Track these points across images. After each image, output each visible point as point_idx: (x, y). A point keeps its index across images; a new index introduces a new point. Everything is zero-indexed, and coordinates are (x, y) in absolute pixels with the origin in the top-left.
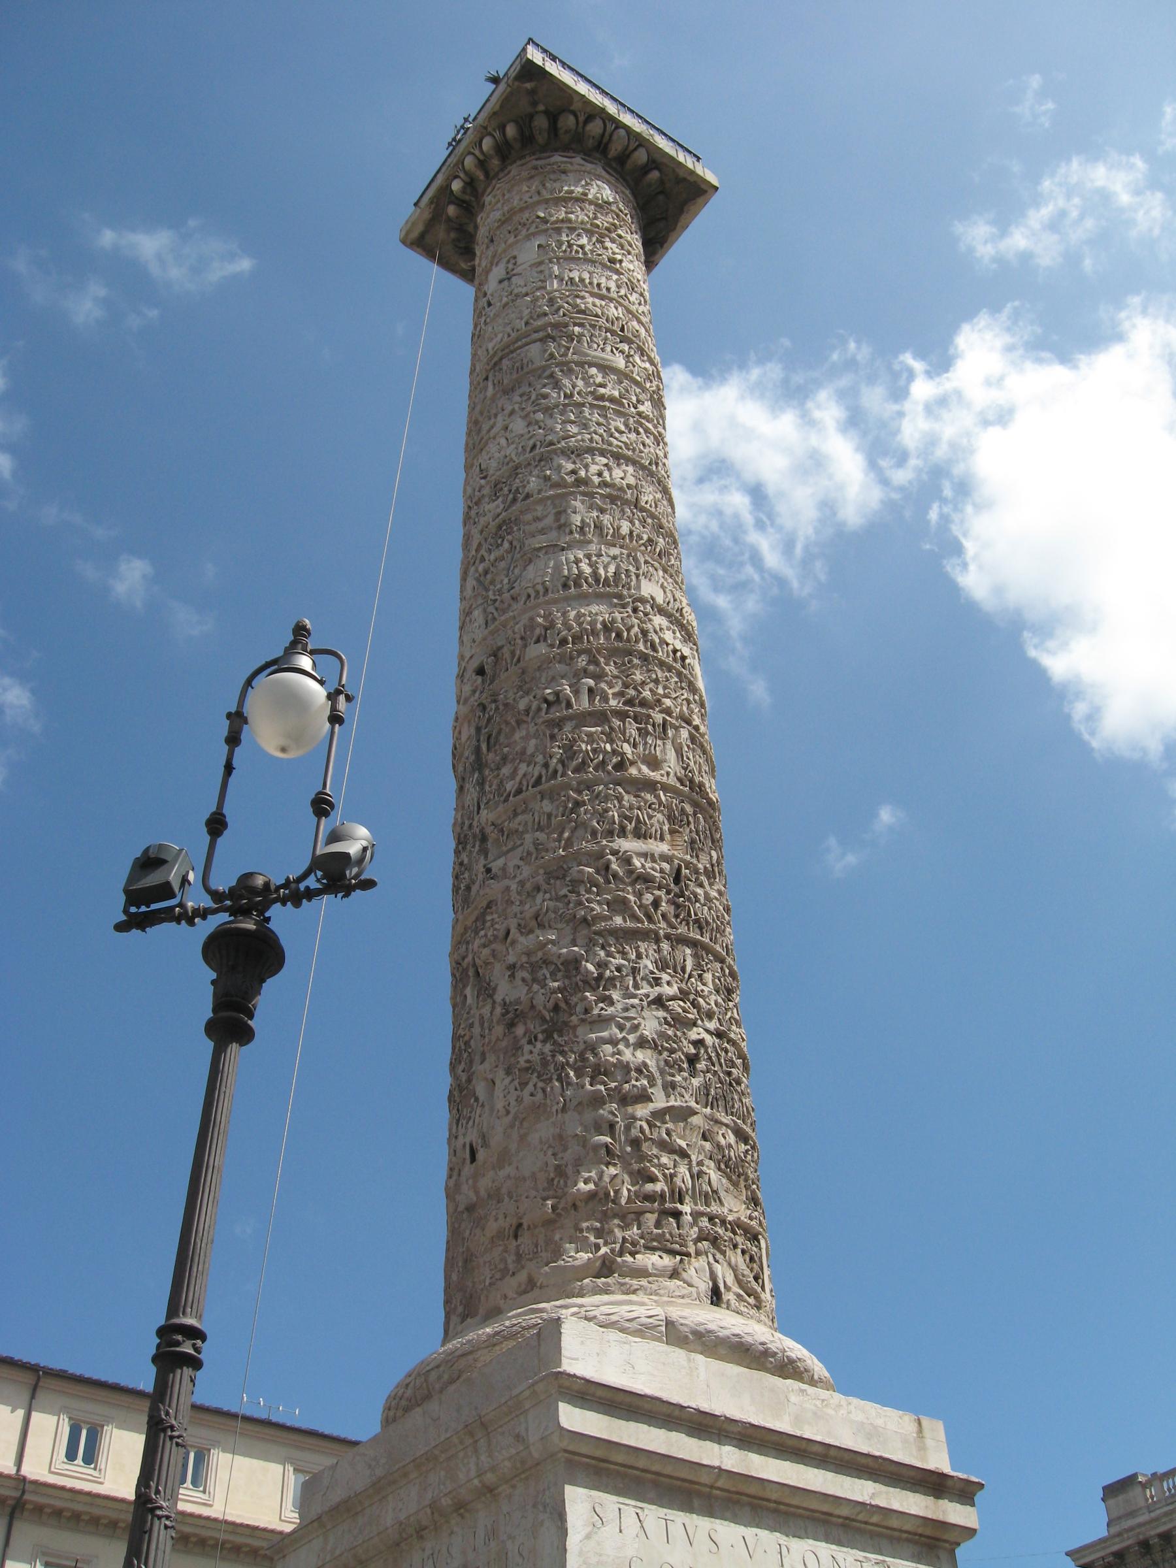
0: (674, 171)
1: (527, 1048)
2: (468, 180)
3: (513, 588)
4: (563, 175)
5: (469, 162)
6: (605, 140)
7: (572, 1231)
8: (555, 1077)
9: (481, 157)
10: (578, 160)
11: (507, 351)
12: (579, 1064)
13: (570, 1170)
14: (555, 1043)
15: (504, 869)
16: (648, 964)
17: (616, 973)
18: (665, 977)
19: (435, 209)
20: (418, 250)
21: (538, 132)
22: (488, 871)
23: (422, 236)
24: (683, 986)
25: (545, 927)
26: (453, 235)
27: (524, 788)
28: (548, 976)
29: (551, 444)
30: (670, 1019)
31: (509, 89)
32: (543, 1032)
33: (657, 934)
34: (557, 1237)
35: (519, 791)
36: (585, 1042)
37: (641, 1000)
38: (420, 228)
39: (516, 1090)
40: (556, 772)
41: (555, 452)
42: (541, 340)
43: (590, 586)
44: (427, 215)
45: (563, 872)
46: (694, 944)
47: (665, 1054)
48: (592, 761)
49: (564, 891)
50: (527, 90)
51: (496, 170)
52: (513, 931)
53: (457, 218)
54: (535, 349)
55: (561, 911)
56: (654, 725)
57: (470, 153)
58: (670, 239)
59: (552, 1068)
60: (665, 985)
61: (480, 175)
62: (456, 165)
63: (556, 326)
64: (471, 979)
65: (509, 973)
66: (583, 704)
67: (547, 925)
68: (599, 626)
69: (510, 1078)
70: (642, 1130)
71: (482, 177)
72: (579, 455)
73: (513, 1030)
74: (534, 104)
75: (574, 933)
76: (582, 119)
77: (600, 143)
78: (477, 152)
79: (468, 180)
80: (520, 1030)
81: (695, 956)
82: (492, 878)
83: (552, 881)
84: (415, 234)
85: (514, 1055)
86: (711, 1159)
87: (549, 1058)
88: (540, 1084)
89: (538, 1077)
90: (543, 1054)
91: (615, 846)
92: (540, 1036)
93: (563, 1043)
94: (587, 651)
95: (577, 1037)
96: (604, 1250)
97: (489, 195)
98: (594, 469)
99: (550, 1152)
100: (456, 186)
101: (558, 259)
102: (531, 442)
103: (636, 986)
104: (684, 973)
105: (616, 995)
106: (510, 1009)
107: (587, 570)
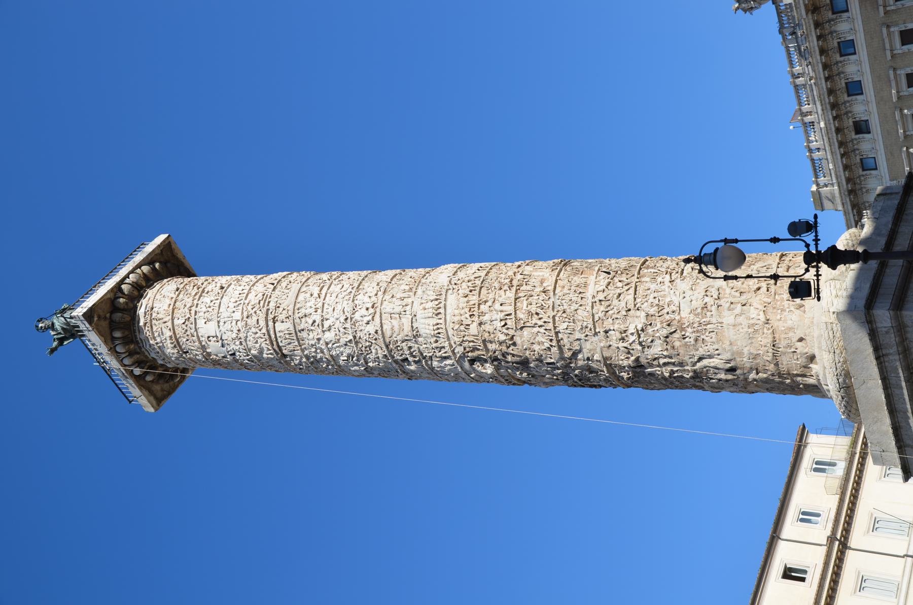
0: (156, 255)
1: (687, 339)
2: (137, 364)
3: (430, 342)
4: (154, 310)
5: (126, 361)
6: (135, 286)
7: (781, 322)
8: (705, 327)
9: (127, 354)
10: (144, 301)
11: (275, 343)
12: (700, 317)
13: (752, 322)
14: (688, 327)
15: (590, 350)
16: (653, 287)
17: (657, 299)
18: (659, 279)
19: (144, 388)
20: (162, 403)
21: (123, 320)
22: (588, 359)
23: (156, 398)
24: (664, 273)
25: (626, 330)
26: (161, 382)
27: (551, 338)
28: (653, 329)
29: (346, 319)
30: (682, 279)
31: (95, 330)
32: (681, 332)
33: (637, 282)
34: (783, 329)
35: (551, 340)
36: (690, 314)
37: (671, 289)
38: (152, 398)
39: (707, 346)
40: (545, 322)
41: (351, 319)
42: (274, 323)
43: (440, 303)
44: (147, 393)
45: (600, 320)
46: (640, 269)
47: (698, 281)
48: (542, 305)
49: (610, 320)
50: (97, 320)
51: (136, 347)
52: (625, 345)
53: (154, 375)
54: (279, 326)
55: (621, 322)
56: (524, 279)
57: (122, 360)
58: (188, 267)
59: (700, 328)
60: (665, 279)
61: (136, 357)
62: (125, 370)
63: (267, 314)
64: (642, 370)
65: (646, 348)
66: (509, 309)
67: (626, 329)
68: (466, 299)
69: (700, 349)
70: (737, 291)
71: (138, 356)
72: (356, 307)
73: (676, 347)
74: (105, 318)
75: (633, 317)
76: (120, 295)
77: (136, 288)
78: (124, 356)
79: (137, 364)
80: (677, 344)
81: (648, 268)
82: (593, 357)
83: (604, 326)
84: (154, 402)
85: (689, 347)
86: (750, 267)
87: (695, 330)
88: (707, 334)
89: (703, 334)
90: (692, 333)
91: (590, 297)
92: (683, 333)
93: (689, 323)
94: (479, 304)
95: (686, 318)
96: (792, 308)
97: (149, 354)
98: (366, 299)
99: (741, 330)
100: (137, 371)
101: (218, 313)
102: (342, 330)
103: (664, 291)
104: (657, 272)
105: (668, 300)
106: (665, 348)
107: (430, 305)
